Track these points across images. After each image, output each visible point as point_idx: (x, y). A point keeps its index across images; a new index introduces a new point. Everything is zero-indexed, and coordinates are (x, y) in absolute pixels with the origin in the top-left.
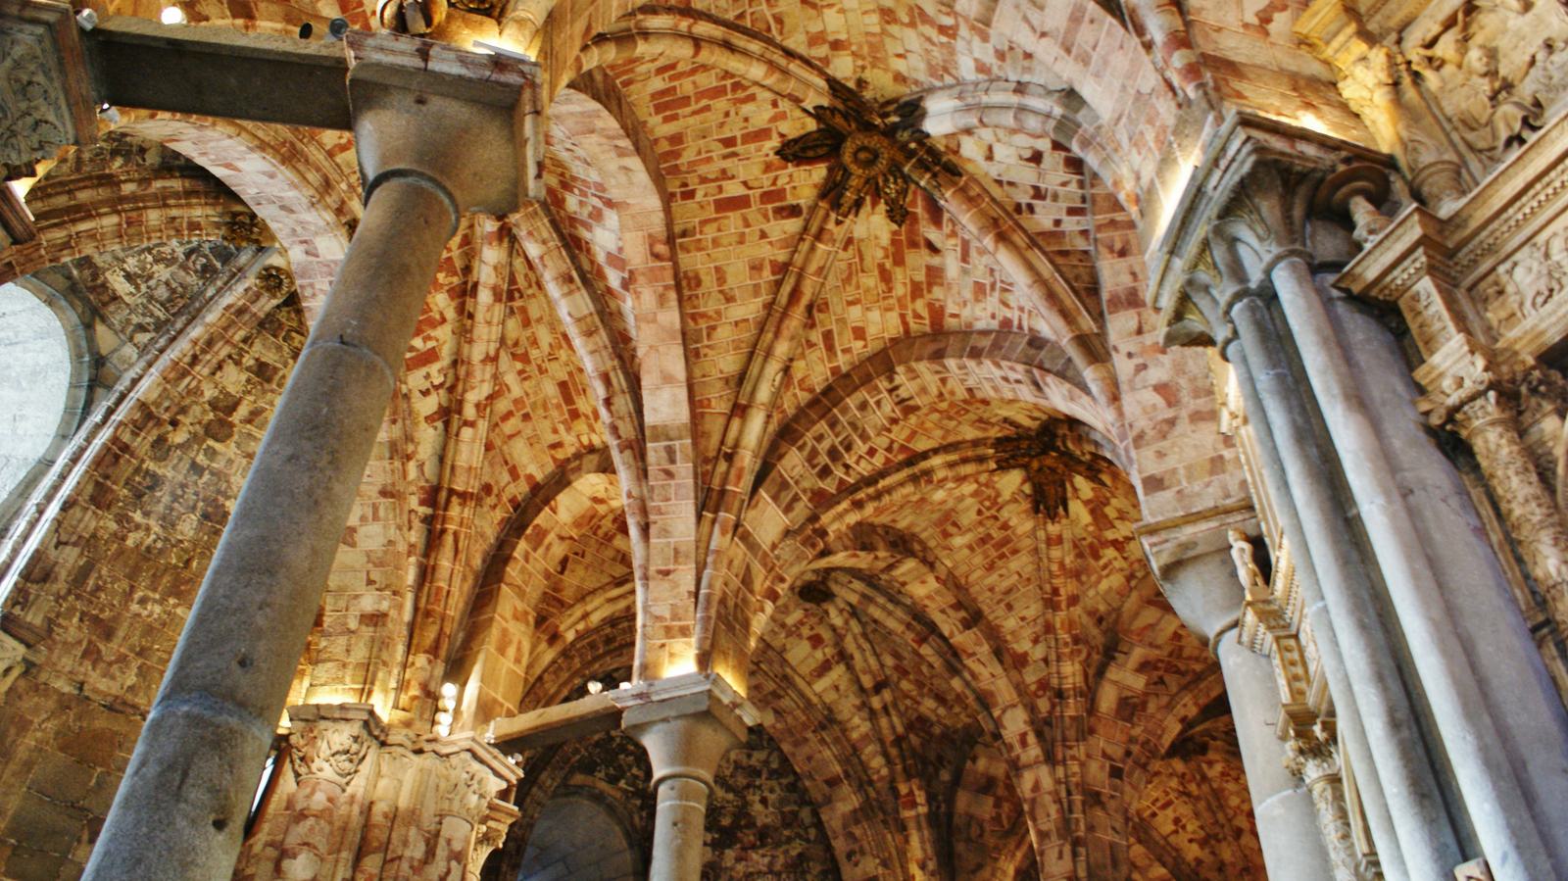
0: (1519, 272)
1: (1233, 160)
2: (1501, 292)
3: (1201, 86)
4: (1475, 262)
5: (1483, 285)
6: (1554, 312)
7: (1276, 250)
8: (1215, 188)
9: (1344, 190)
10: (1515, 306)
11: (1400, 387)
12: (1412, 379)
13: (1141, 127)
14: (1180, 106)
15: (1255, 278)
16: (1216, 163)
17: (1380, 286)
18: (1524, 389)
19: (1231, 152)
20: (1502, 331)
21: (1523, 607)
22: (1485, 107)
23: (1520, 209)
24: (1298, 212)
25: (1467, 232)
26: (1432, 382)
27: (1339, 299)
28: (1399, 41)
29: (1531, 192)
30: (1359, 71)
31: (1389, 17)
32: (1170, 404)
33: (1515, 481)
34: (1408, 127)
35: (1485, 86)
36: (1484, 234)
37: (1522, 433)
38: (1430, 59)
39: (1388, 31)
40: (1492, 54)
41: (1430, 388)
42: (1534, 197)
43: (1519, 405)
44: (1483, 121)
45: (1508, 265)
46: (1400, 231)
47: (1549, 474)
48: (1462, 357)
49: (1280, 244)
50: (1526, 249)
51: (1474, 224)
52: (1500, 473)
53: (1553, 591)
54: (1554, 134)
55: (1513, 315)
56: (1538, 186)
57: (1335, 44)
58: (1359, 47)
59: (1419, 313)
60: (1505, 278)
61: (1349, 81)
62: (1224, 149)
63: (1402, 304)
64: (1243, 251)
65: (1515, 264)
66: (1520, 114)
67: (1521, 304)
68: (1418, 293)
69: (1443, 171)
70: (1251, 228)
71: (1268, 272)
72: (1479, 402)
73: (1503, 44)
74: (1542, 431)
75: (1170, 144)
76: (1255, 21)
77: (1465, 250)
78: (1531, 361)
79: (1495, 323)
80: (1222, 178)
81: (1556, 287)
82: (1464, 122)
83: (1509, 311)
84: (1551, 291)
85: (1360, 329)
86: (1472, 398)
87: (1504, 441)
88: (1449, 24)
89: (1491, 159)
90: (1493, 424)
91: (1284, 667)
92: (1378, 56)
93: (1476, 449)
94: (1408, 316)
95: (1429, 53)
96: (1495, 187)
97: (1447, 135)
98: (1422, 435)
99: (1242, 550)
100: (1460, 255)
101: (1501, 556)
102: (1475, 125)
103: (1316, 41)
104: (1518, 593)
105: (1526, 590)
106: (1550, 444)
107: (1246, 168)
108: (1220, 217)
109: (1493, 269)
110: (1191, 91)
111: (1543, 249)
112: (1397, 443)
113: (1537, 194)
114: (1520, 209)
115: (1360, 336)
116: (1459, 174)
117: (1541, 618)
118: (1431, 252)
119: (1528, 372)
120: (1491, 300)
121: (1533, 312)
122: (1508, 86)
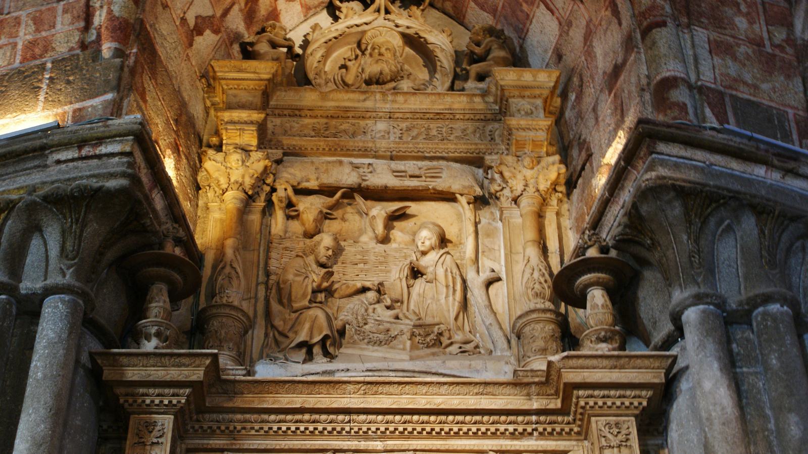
1: (99, 157)
3: (119, 53)
4: (212, 433)
7: (68, 279)
8: (59, 162)
9: (162, 270)
13: (23, 14)
14: (83, 46)
15: (29, 284)
16: (81, 143)
17: (130, 390)
19: (103, 149)
22: (304, 295)
24: (110, 255)
25: (231, 405)
28: (279, 162)
29: (299, 417)
30: (235, 158)
31: (285, 133)
34: (236, 250)
35: (316, 276)
36: (239, 416)
38: (290, 205)
39: (278, 145)
40: (338, 251)
42: (297, 422)
44: (296, 305)
46: (186, 361)
49: (77, 275)
51: (239, 402)
54: (350, 387)
56: (307, 417)
57: (237, 115)
58: (250, 138)
59: (144, 444)
61: (219, 156)
62: (100, 140)
64: (35, 243)
66: (326, 331)
68: (155, 424)
69: (240, 321)
70: (63, 233)
71: (49, 291)
73: (350, 251)
75: (42, 68)
76: (192, 22)
77: (214, 416)
80: (73, 160)
82: (279, 290)
88: (327, 191)
89: (277, 343)
92: (258, 162)
94: (131, 439)
95: (294, 199)
97: (257, 284)
100: (207, 416)
102: (285, 301)
103: (219, 90)
107: (112, 184)
108: (45, 198)
110: (107, 48)
113: (301, 421)
116: (246, 332)
122: (329, 292)
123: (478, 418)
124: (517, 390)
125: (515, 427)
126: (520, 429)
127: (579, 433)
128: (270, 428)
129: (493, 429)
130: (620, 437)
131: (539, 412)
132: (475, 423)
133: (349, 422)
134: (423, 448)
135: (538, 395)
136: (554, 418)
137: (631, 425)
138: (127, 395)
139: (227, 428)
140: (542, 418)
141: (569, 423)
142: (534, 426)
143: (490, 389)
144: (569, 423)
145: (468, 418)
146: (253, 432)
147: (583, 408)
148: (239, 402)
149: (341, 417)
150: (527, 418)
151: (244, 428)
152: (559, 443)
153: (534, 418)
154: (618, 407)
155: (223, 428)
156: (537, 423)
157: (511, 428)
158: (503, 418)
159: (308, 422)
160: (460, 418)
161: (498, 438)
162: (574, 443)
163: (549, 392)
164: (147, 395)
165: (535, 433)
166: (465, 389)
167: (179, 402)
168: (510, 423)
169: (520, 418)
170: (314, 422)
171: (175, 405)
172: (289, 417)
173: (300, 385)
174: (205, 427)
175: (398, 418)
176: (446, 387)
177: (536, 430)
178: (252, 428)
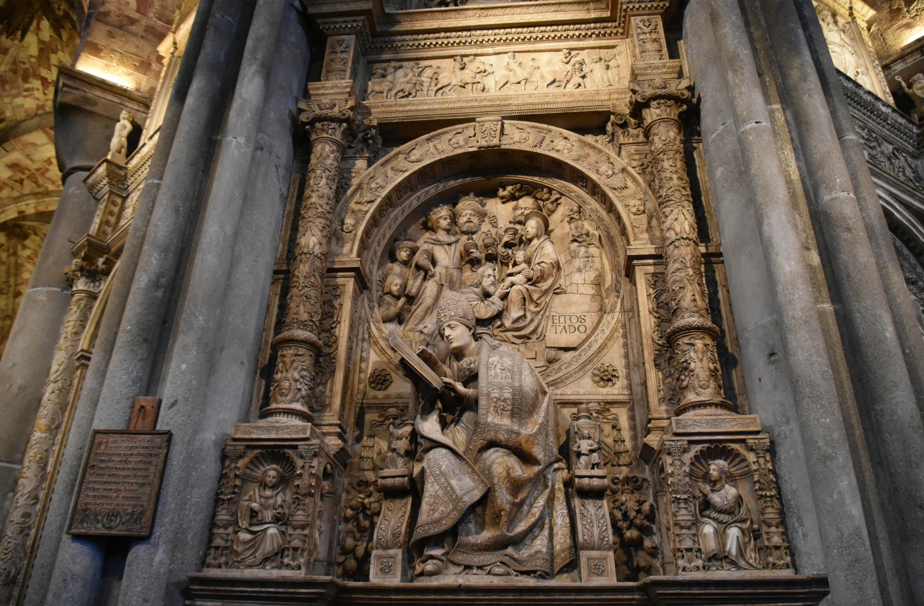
0: (400, 73)
2: (384, 76)
5: (377, 65)
6: (405, 105)
10: (386, 89)
11: (295, 86)
12: (306, 86)
18: (360, 135)
20: (370, 97)
21: (278, 256)
23: (425, 39)
26: (316, 95)
27: (297, 9)
29: (437, 35)
32: (138, 11)
33: (324, 181)
36: (399, 38)
37: (344, 158)
41: (312, 98)
43: (352, 142)
45: (397, 64)
47: (342, 190)
48: (343, 93)
50: (412, 63)
51: (398, 28)
52: (319, 172)
53: (303, 256)
54: (470, 13)
55: (382, 93)
56: (442, 34)
60: (390, 70)
63: (330, 39)
65: (401, 67)
67: (390, 90)
72: (333, 125)
74: (354, 165)
77: (383, 39)
78: (375, 123)
79: (369, 91)
81: (414, 94)
83: (381, 89)
84: (410, 94)
85: (295, 35)
86: (333, 120)
87: (332, 156)
90: (334, 142)
91: (104, 212)
93: (314, 150)
96: (422, 16)
98: (289, 122)
99: (124, 127)
100: (379, 39)
101: (285, 219)
104: (281, 245)
105: (286, 248)
106: (353, 175)
109: (389, 61)
111: (421, 69)
112: (272, 116)
113: (439, 38)
114: (425, 39)
115: (293, 40)
117: (284, 267)
118: (366, 23)
119: (370, 127)
120: (375, 76)
121: (393, 99)
123: (555, 28)
124: (580, 7)
125: (580, 32)
126: (583, 33)
127: (622, 34)
128: (419, 44)
129: (565, 34)
130: (651, 27)
131: (596, 20)
132: (553, 31)
133: (470, 36)
134: (519, 50)
135: (595, 9)
136: (605, 24)
137: (658, 21)
138: (324, 23)
139: (392, 46)
140: (598, 25)
141: (616, 27)
142: (592, 31)
143: (562, 7)
144: (616, 27)
145: (548, 28)
146: (409, 47)
147: (625, 11)
148: (398, 28)
149: (465, 33)
150: (588, 26)
151: (403, 45)
152: (609, 41)
153: (592, 25)
154: (649, 8)
155: (389, 46)
156: (594, 28)
157: (577, 33)
158: (572, 27)
159: (443, 38)
160: (543, 28)
161: (569, 40)
162: (620, 41)
163: (602, 7)
164: (337, 22)
165: (593, 36)
166: (546, 8)
167: (358, 26)
168: (576, 30)
169: (583, 26)
170: (447, 38)
171: (355, 28)
172: (431, 36)
173: (437, 14)
174: (378, 46)
175: (502, 31)
176: (533, 8)
177: (593, 33)
178: (408, 45)
